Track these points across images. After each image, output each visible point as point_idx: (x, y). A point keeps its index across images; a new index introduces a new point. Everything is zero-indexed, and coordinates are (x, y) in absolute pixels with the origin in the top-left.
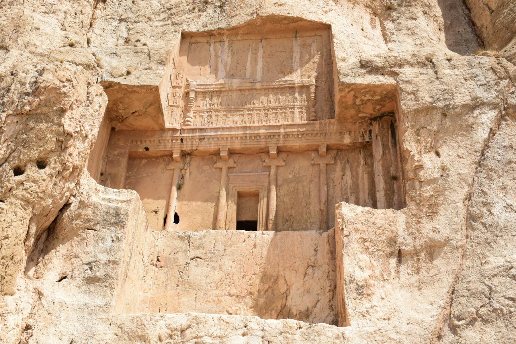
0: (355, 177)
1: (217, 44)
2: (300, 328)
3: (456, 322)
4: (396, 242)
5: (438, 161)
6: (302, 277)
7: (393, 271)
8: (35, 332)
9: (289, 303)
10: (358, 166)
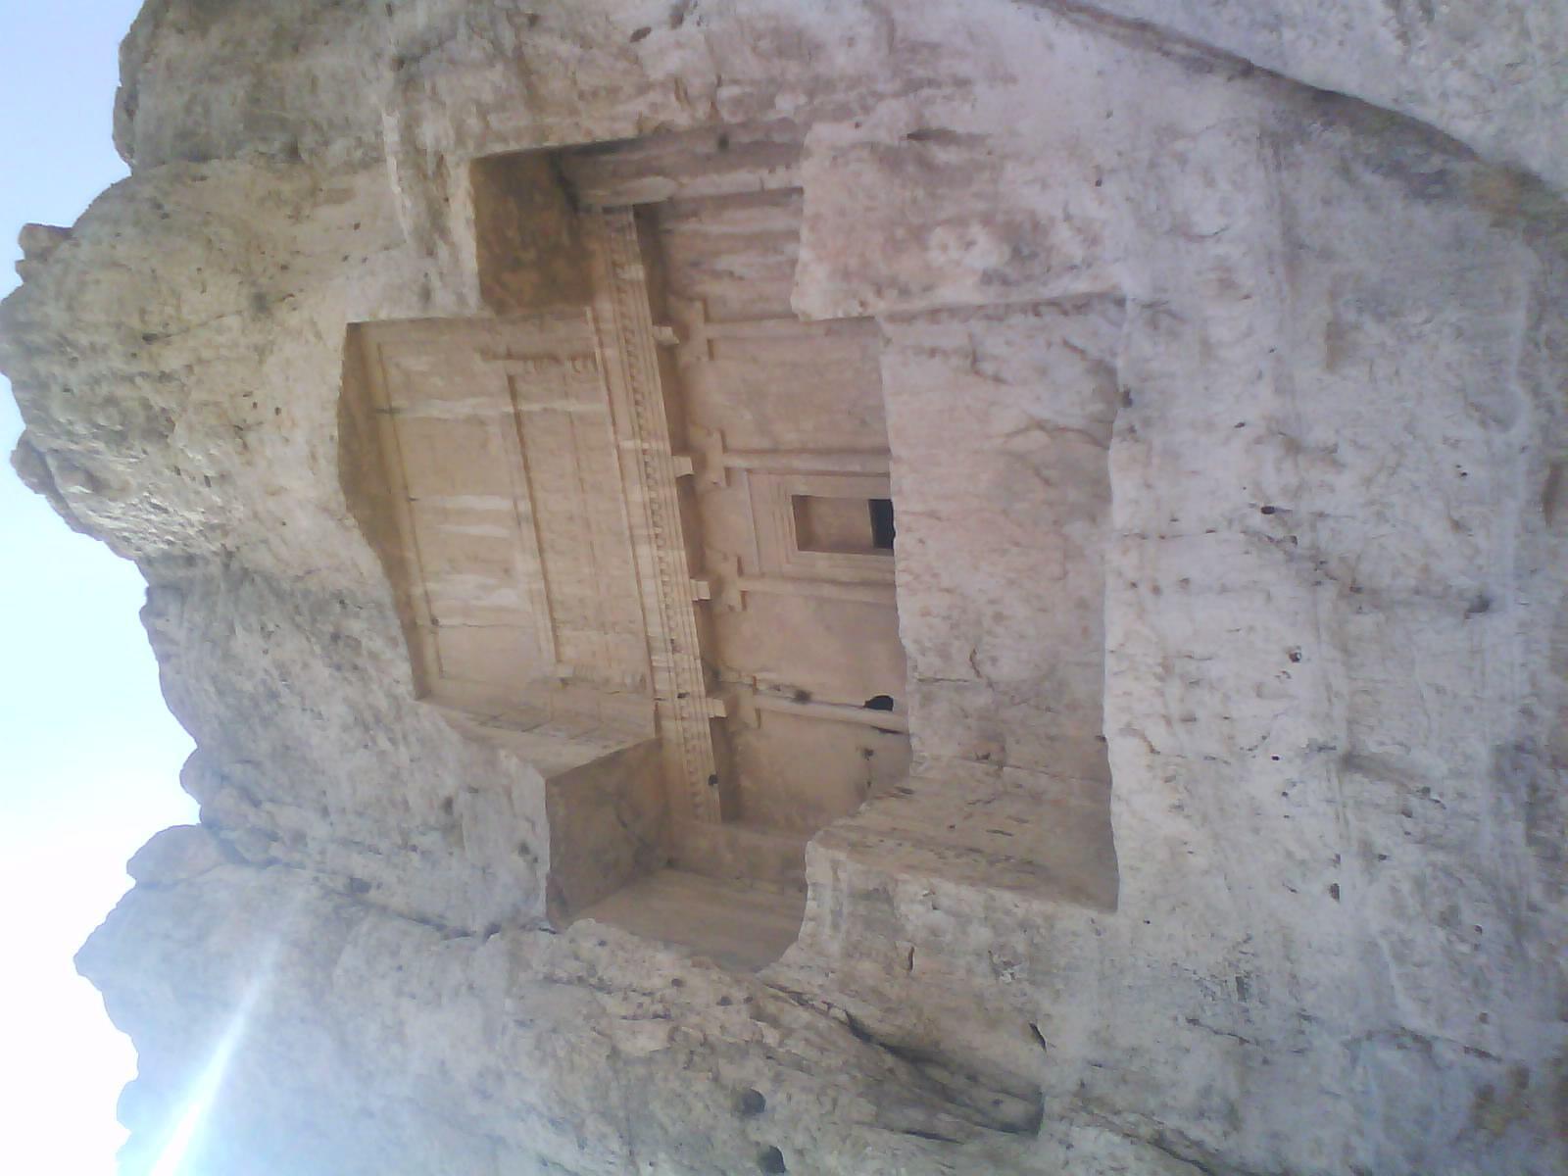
2: (1132, 430)
5: (660, 36)
8: (1172, 1122)
9: (1076, 422)
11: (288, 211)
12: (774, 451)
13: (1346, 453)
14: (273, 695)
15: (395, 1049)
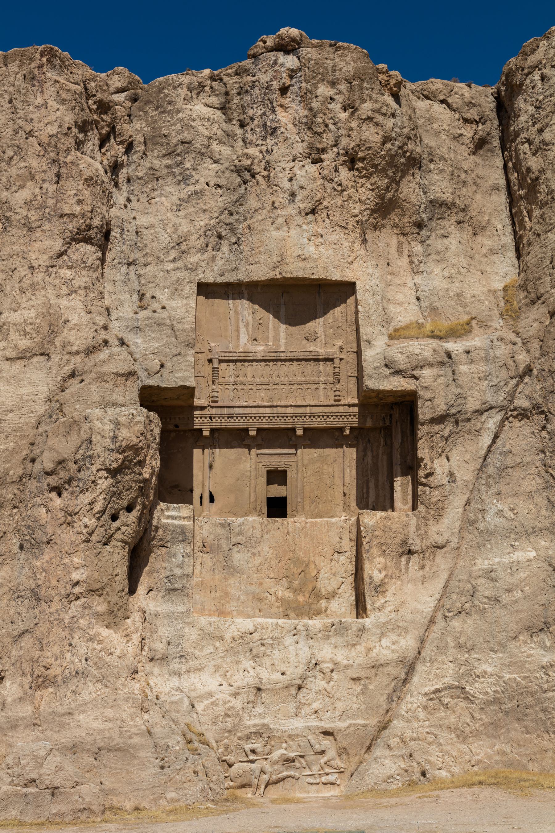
3: (447, 614)
4: (407, 543)
7: (403, 567)
9: (318, 584)
13: (332, 683)
14: (185, 179)
15: (65, 290)
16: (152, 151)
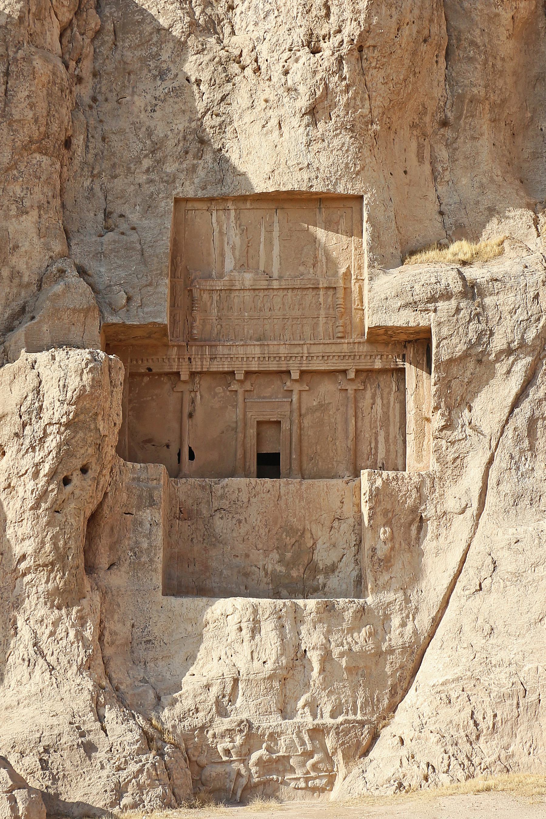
0: (386, 406)
1: (221, 213)
6: (329, 530)
9: (315, 557)
10: (389, 393)
11: (417, 121)
12: (300, 415)
14: (162, 75)
16: (123, 41)
